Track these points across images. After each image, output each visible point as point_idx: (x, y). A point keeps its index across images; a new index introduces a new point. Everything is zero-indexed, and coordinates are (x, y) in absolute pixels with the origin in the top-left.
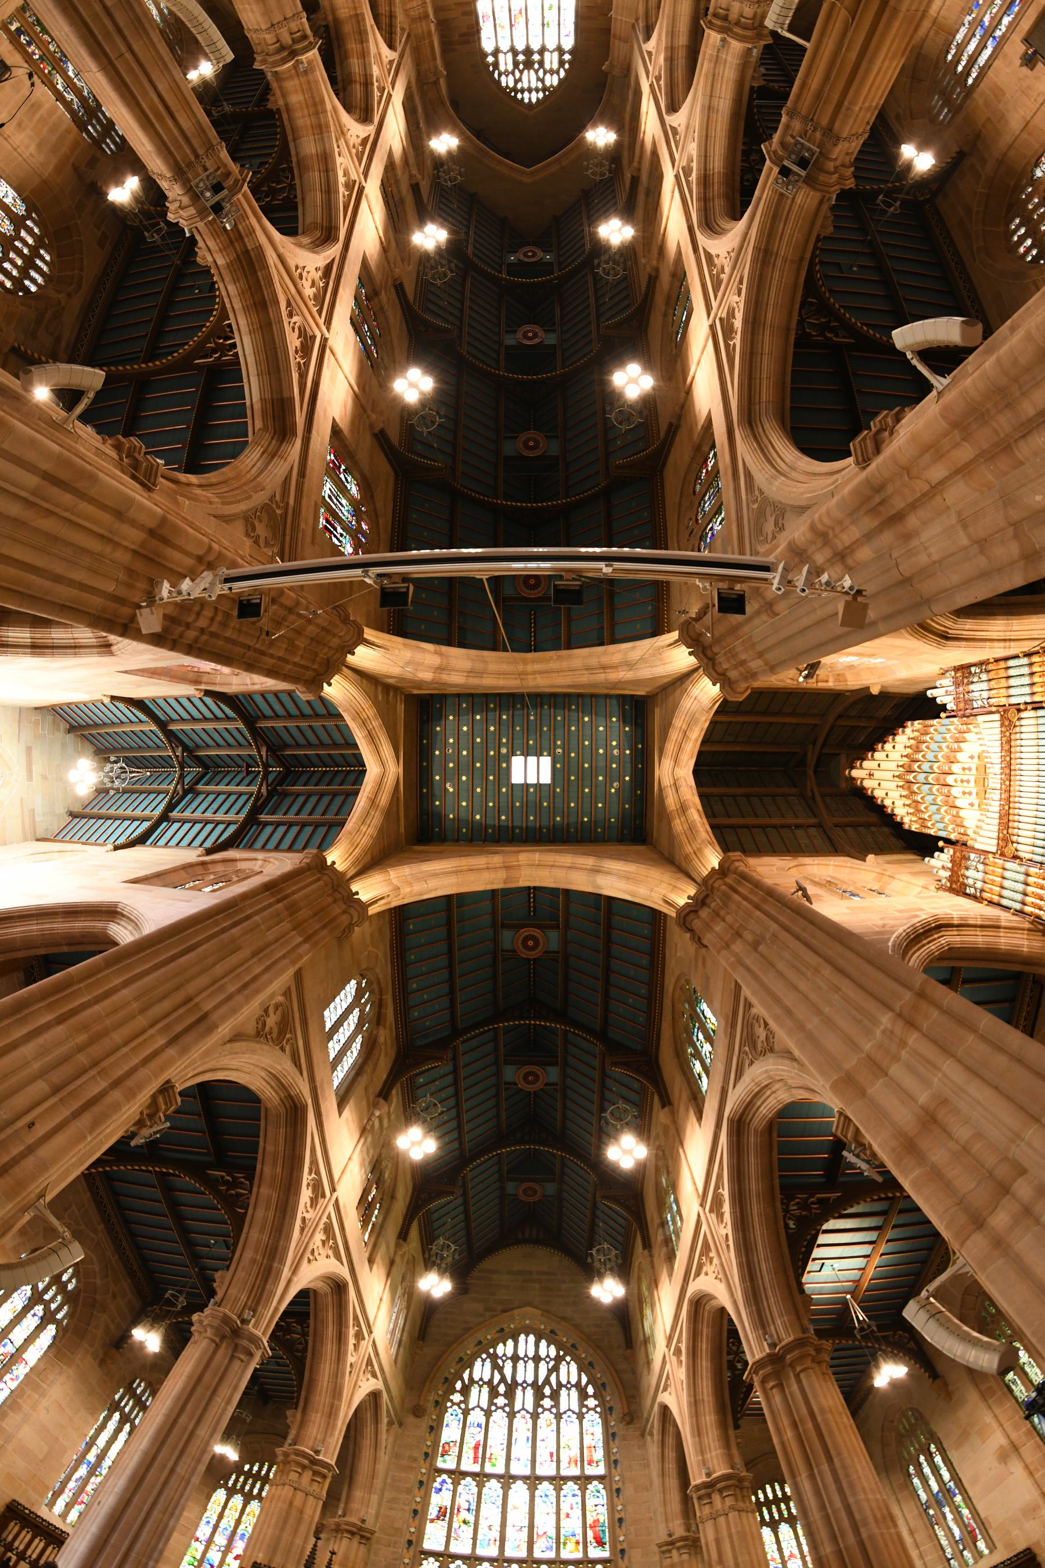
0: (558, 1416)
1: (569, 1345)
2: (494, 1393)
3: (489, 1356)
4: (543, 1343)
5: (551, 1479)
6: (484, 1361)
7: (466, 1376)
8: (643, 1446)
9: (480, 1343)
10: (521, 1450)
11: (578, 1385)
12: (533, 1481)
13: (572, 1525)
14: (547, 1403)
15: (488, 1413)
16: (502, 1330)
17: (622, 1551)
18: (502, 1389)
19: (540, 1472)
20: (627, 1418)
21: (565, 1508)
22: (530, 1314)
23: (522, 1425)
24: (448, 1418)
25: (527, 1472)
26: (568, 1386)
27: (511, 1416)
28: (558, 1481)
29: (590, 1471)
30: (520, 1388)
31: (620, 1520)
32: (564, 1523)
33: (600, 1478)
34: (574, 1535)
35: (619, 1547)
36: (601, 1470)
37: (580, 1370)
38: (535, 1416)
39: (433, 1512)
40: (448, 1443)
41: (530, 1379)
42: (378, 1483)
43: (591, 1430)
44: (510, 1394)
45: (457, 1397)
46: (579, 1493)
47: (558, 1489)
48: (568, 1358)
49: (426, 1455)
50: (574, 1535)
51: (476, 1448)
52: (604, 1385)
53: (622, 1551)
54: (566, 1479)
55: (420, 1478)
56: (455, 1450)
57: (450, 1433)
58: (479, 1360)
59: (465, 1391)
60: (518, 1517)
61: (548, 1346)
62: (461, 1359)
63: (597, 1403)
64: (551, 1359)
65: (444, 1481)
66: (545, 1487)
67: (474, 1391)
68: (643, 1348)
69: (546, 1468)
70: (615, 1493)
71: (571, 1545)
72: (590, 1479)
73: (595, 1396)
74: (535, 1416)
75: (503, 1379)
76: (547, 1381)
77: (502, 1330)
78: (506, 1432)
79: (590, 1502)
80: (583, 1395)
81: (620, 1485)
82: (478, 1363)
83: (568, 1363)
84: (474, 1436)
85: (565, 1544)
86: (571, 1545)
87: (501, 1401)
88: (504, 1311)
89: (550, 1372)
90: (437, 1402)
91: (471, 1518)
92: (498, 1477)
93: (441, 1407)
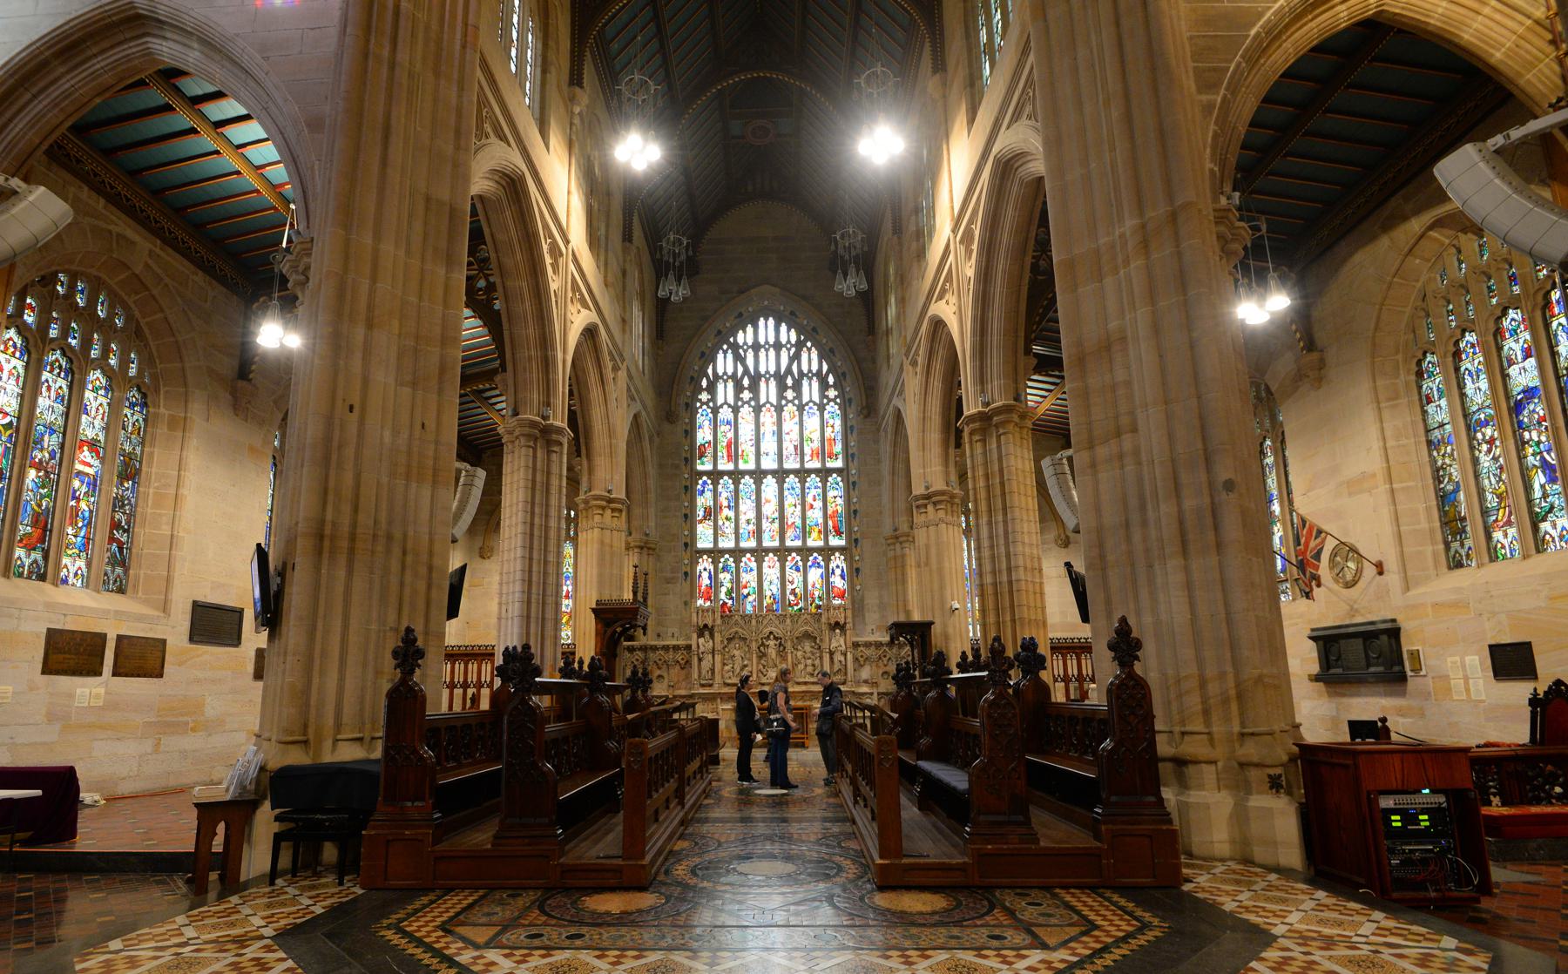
0: (801, 408)
1: (809, 329)
2: (739, 388)
4: (784, 327)
5: (795, 472)
6: (725, 352)
7: (710, 371)
8: (877, 441)
10: (769, 445)
11: (819, 374)
12: (781, 474)
13: (815, 515)
14: (790, 394)
15: (736, 410)
17: (856, 541)
18: (746, 382)
19: (787, 466)
20: (865, 412)
21: (809, 499)
23: (768, 418)
24: (700, 419)
25: (775, 466)
26: (810, 375)
27: (757, 410)
28: (803, 474)
29: (831, 464)
30: (763, 379)
31: (855, 512)
32: (809, 513)
33: (838, 471)
34: (817, 525)
35: (854, 537)
36: (839, 464)
37: (821, 357)
38: (779, 409)
39: (701, 513)
41: (772, 370)
42: (652, 496)
43: (831, 422)
44: (754, 388)
45: (704, 396)
46: (820, 484)
47: (803, 482)
48: (809, 344)
49: (686, 459)
50: (817, 525)
51: (729, 446)
52: (844, 374)
53: (856, 541)
54: (810, 472)
55: (684, 483)
56: (710, 451)
57: (703, 435)
58: (721, 352)
59: (712, 389)
60: (770, 509)
61: (789, 330)
62: (703, 354)
63: (836, 393)
64: (792, 346)
65: (705, 483)
66: (792, 479)
67: (720, 387)
68: (885, 338)
69: (791, 463)
70: (850, 487)
71: (815, 535)
72: (830, 471)
73: (835, 386)
74: (779, 409)
75: (746, 371)
76: (789, 371)
78: (753, 427)
79: (831, 494)
80: (824, 386)
81: (856, 479)
82: (720, 356)
83: (809, 350)
84: (726, 433)
85: (810, 533)
86: (815, 535)
87: (746, 395)
89: (791, 360)
90: (687, 404)
91: (731, 514)
92: (750, 473)
93: (692, 412)
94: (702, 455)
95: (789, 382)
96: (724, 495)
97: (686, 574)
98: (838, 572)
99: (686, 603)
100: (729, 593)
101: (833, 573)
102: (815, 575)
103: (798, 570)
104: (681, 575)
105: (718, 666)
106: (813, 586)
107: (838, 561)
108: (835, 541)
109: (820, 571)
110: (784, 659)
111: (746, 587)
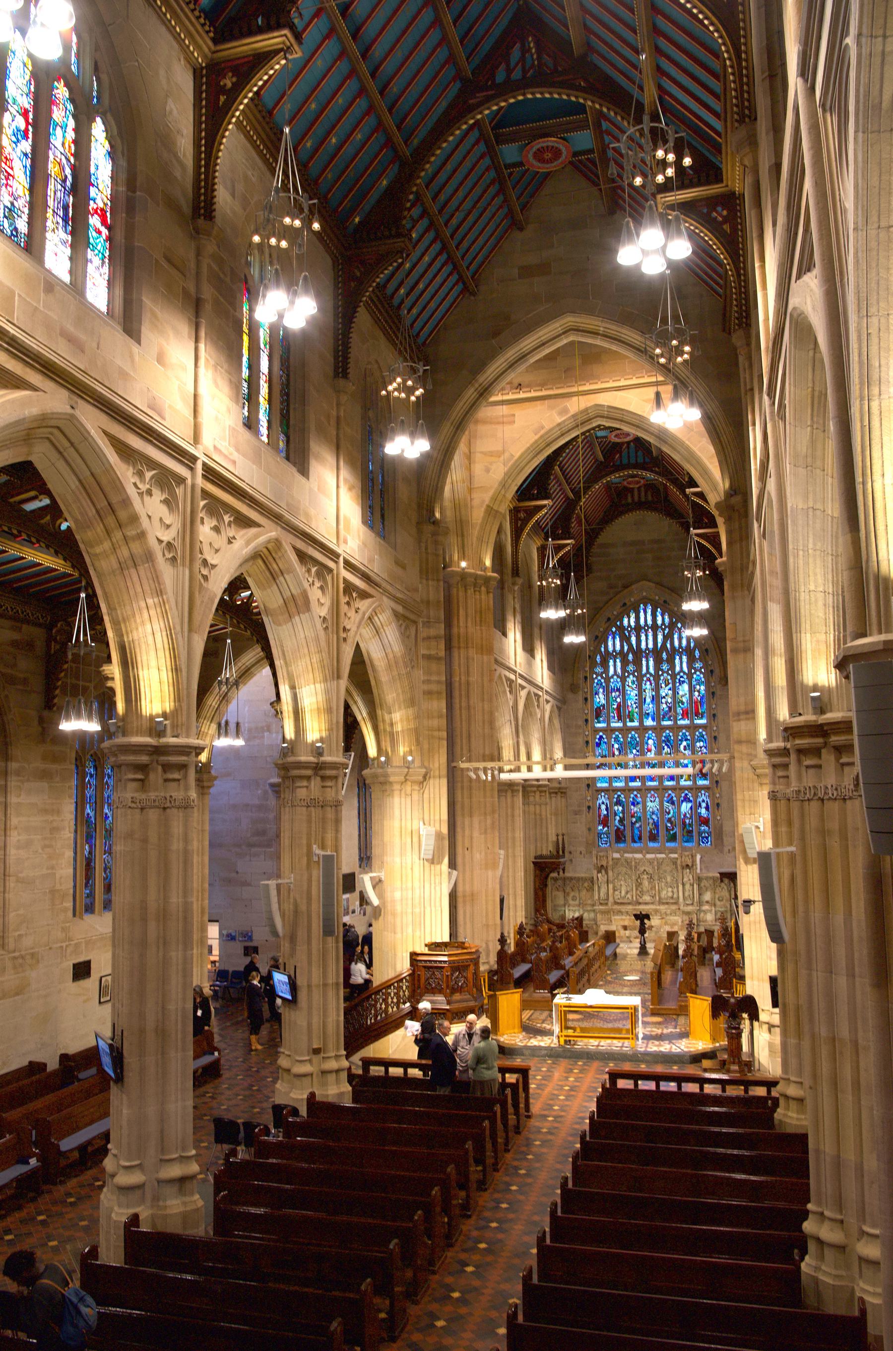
0: (674, 676)
2: (625, 662)
3: (618, 628)
9: (609, 619)
15: (623, 679)
16: (625, 604)
21: (682, 747)
22: (645, 588)
29: (698, 722)
36: (703, 721)
40: (598, 708)
41: (651, 646)
44: (637, 663)
45: (599, 670)
53: (717, 782)
61: (663, 615)
73: (700, 659)
74: (657, 677)
77: (625, 604)
80: (691, 660)
87: (631, 668)
88: (626, 587)
89: (665, 638)
94: (598, 716)
95: (664, 655)
96: (616, 746)
97: (589, 807)
98: (704, 805)
99: (589, 829)
100: (621, 821)
101: (700, 805)
102: (685, 807)
103: (673, 803)
104: (585, 809)
105: (611, 891)
106: (685, 815)
107: (703, 797)
108: (701, 782)
109: (689, 805)
110: (653, 888)
111: (633, 816)
